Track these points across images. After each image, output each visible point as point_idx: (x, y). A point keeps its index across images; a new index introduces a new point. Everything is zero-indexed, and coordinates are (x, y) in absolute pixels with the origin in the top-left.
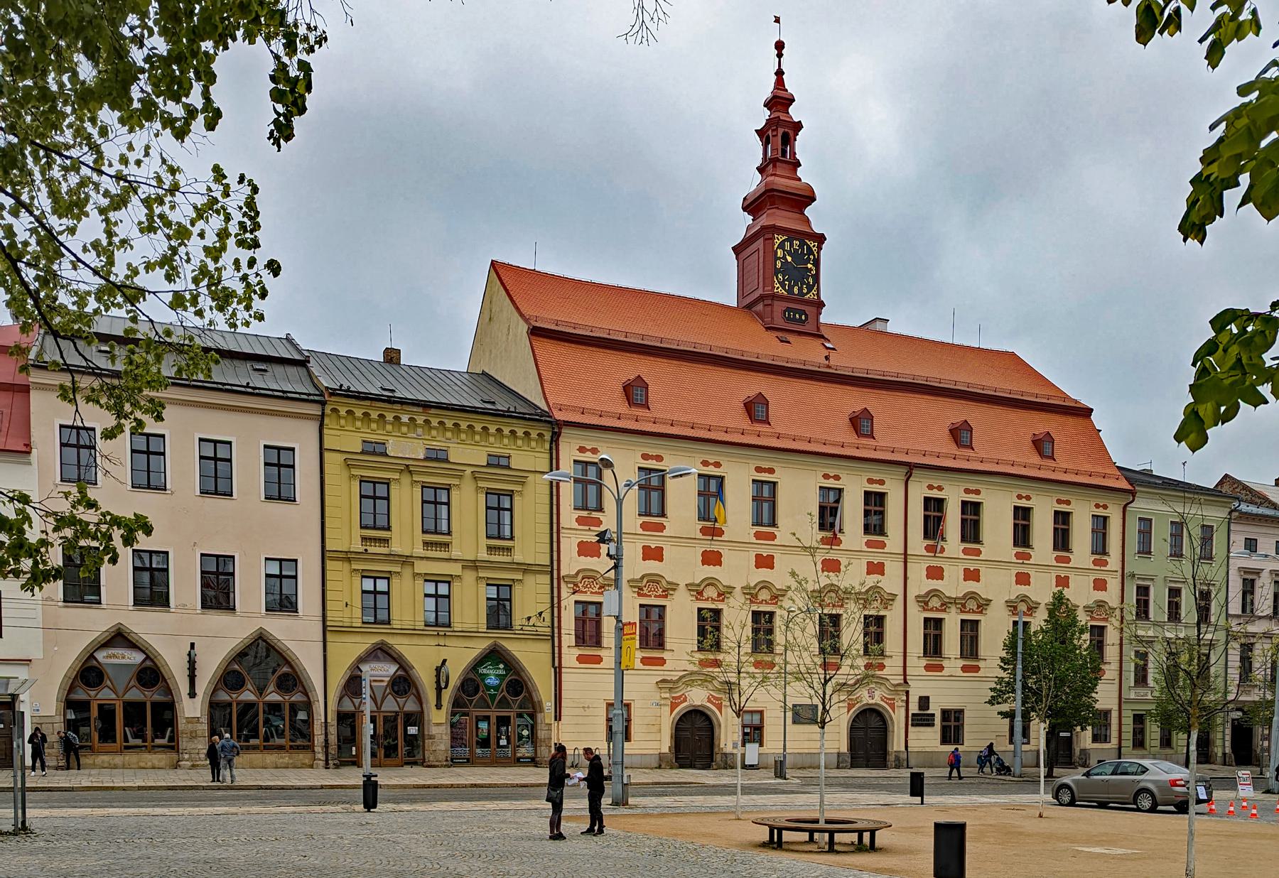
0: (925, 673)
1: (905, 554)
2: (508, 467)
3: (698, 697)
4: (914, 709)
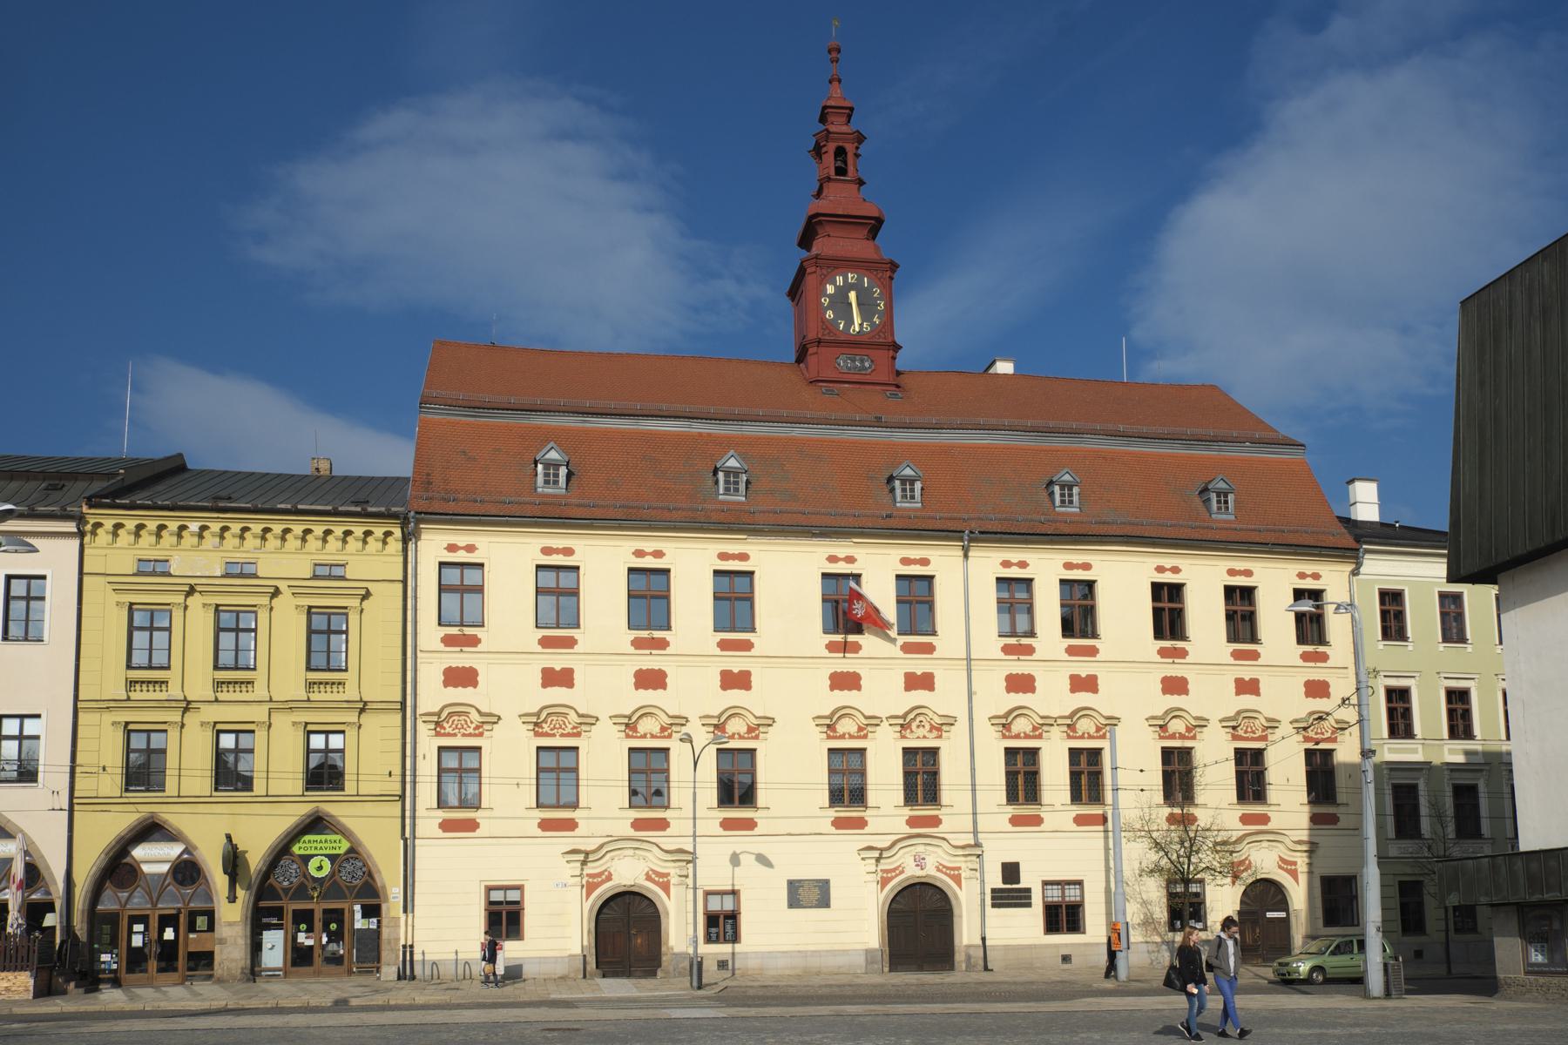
1: (969, 659)
3: (627, 872)
4: (995, 880)
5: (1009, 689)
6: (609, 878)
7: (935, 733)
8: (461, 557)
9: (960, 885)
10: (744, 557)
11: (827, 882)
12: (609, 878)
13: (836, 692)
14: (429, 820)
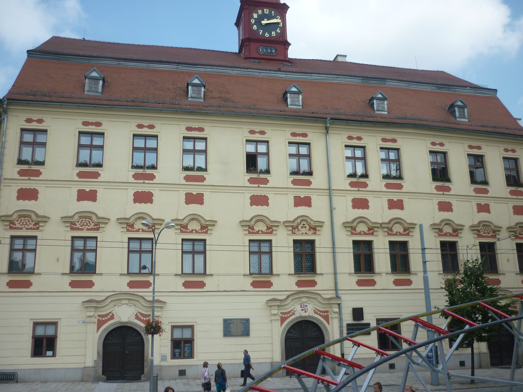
0: (357, 287)
1: (329, 189)
3: (125, 314)
4: (348, 319)
5: (354, 207)
6: (112, 318)
7: (312, 231)
8: (34, 126)
9: (328, 322)
11: (248, 320)
12: (112, 318)
13: (254, 206)
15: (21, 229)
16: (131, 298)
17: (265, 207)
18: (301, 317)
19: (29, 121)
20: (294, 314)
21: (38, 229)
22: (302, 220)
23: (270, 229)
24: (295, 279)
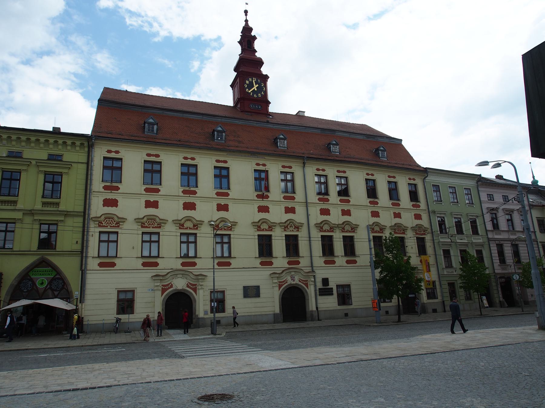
1: (306, 202)
2: (61, 161)
3: (180, 284)
4: (320, 285)
5: (321, 214)
6: (172, 287)
7: (296, 229)
8: (113, 155)
10: (225, 162)
11: (258, 287)
12: (172, 287)
14: (92, 264)
15: (107, 226)
16: (184, 274)
17: (267, 213)
18: (291, 284)
19: (109, 151)
20: (287, 282)
21: (118, 226)
22: (290, 222)
23: (270, 228)
24: (287, 260)
